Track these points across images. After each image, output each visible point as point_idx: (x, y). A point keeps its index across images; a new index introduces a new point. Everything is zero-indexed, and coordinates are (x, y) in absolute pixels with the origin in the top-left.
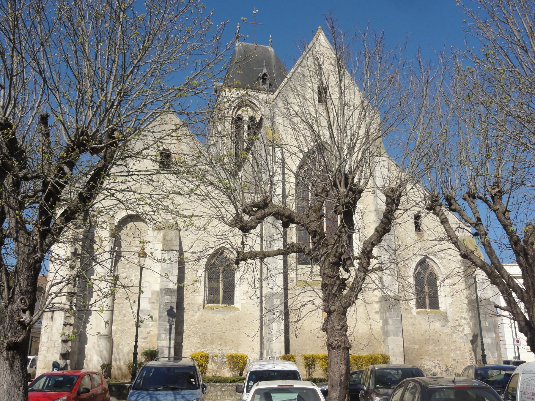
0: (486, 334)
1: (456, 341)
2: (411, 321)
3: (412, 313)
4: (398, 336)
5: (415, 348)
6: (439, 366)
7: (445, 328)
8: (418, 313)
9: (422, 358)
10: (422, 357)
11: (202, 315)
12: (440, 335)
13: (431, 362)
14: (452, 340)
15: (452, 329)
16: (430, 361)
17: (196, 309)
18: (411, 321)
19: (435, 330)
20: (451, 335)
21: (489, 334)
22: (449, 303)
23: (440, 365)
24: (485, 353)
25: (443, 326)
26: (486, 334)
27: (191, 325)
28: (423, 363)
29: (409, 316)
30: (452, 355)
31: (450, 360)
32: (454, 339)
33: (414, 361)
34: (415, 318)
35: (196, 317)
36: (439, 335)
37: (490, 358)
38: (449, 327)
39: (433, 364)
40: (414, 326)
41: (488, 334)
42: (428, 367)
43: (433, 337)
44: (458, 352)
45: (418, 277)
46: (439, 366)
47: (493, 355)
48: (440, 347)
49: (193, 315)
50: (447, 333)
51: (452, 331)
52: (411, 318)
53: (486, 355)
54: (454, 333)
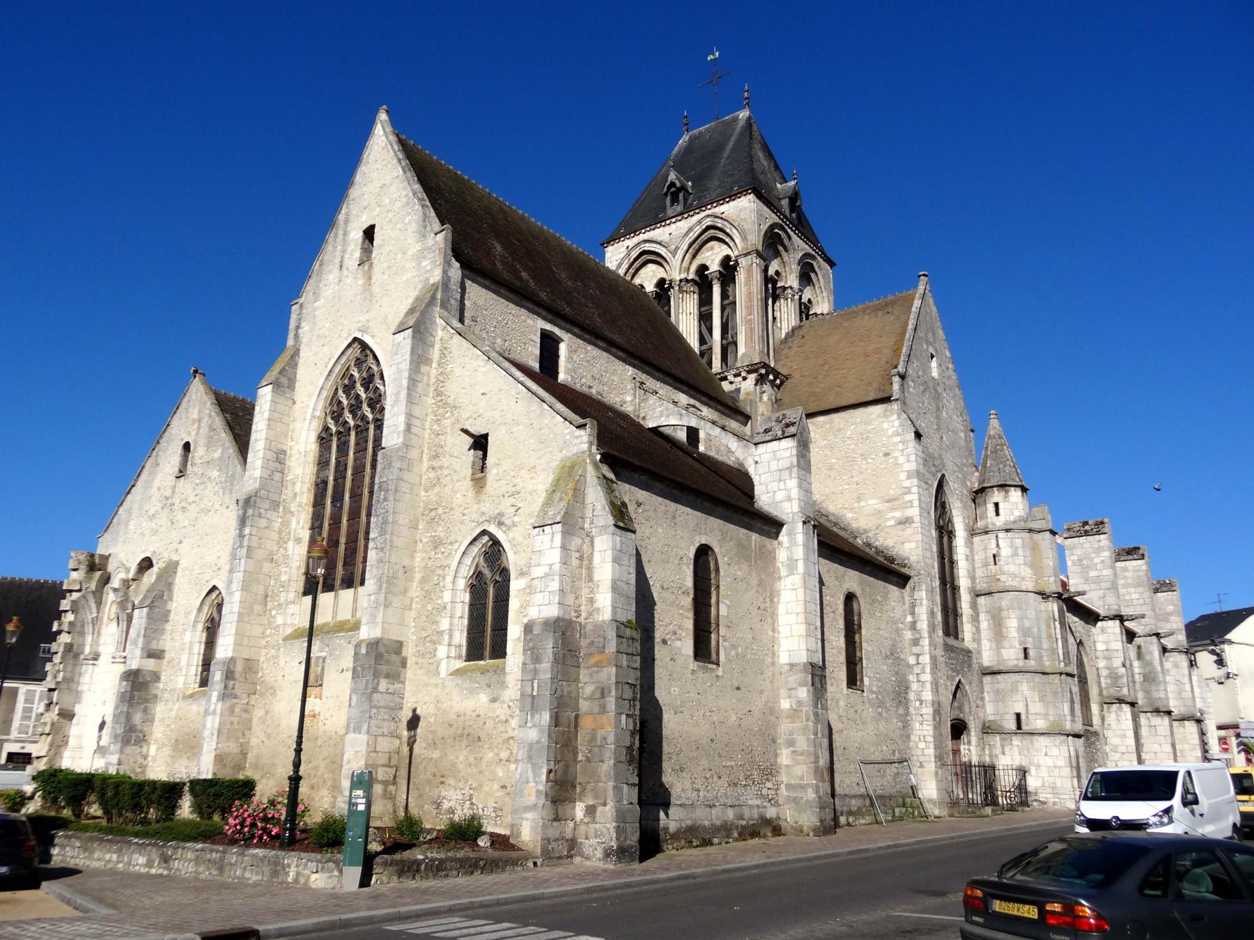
0: (529, 716)
1: (512, 738)
2: (435, 692)
3: (439, 673)
4: (360, 733)
5: (431, 759)
6: (472, 804)
7: (496, 705)
8: (458, 673)
9: (442, 783)
10: (443, 779)
11: (179, 709)
12: (485, 723)
13: (458, 791)
14: (505, 736)
15: (509, 707)
16: (456, 789)
17: (175, 699)
18: (435, 692)
19: (477, 713)
20: (507, 721)
21: (537, 716)
22: (514, 640)
23: (474, 801)
24: (300, 773)
25: (494, 700)
26: (529, 716)
27: (169, 726)
28: (443, 794)
29: (434, 680)
30: (501, 774)
31: (496, 787)
32: (511, 734)
33: (427, 789)
34: (444, 687)
35: (174, 713)
36: (482, 723)
37: (528, 782)
38: (504, 702)
39: (460, 797)
40: (439, 705)
41: (532, 716)
42: (451, 804)
43: (471, 730)
44: (513, 767)
45: (477, 587)
46: (472, 804)
47: (535, 776)
48: (480, 755)
49: (171, 710)
50: (497, 717)
51: (509, 712)
52: (436, 685)
53: (300, 778)
54: (513, 717)
